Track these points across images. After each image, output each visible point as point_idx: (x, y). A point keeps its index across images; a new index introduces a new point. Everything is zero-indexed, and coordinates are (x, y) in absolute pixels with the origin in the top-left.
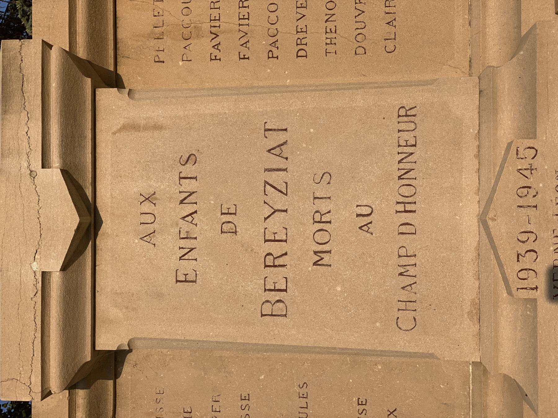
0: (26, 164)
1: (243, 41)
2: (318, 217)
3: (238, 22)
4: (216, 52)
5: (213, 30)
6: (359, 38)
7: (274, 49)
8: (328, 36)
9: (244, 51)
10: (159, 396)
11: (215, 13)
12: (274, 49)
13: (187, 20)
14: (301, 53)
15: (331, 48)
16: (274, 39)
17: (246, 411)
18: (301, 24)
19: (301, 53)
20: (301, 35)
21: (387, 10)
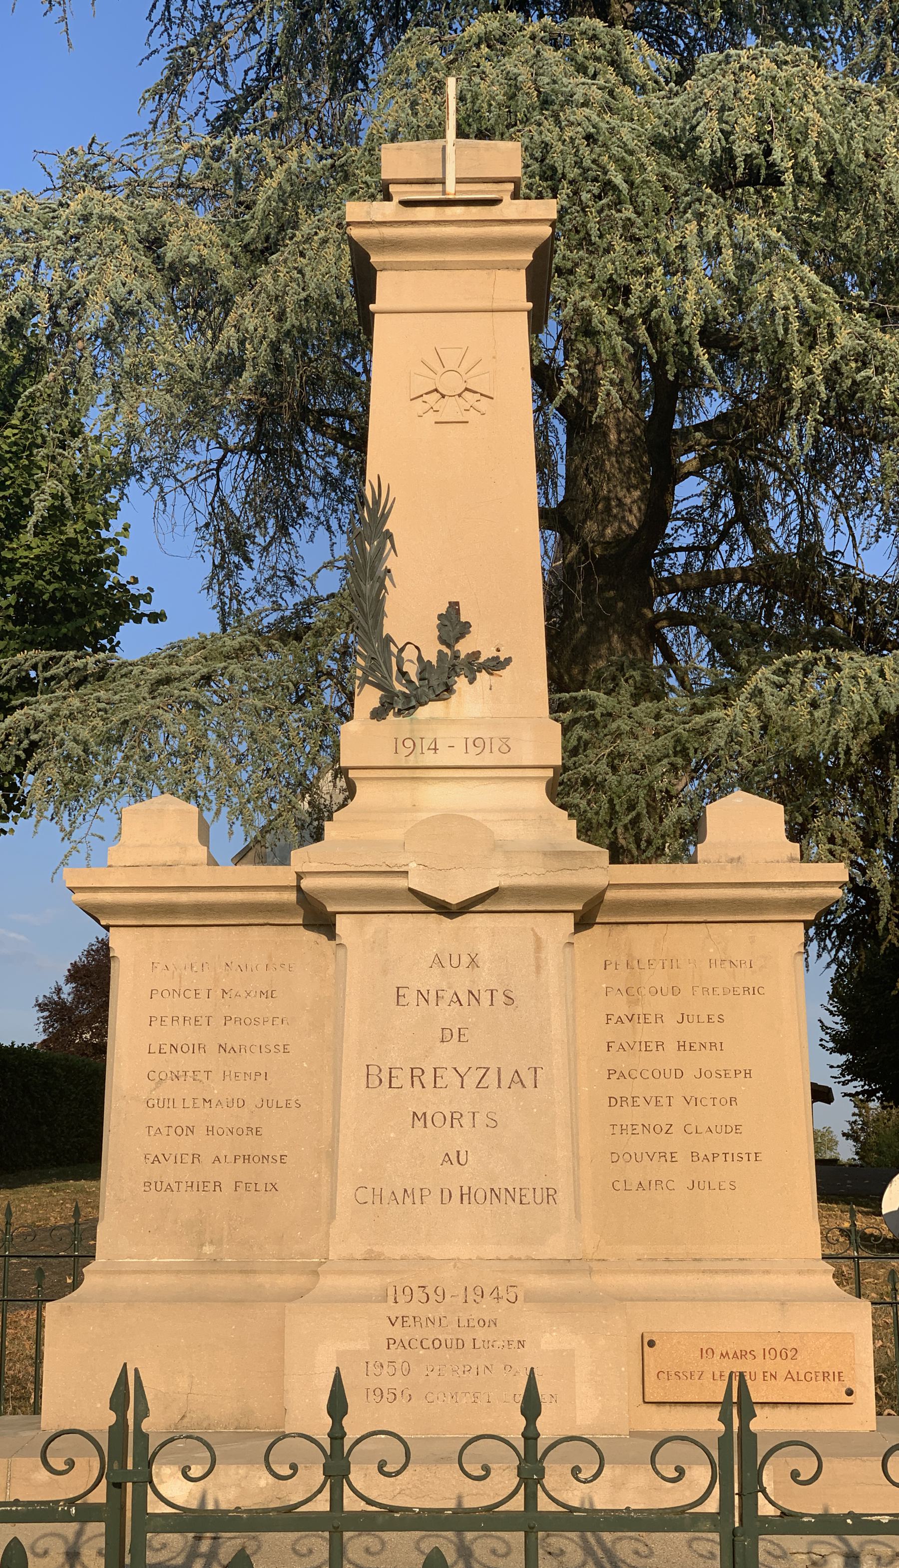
1: (626, 1046)
2: (456, 1116)
3: (643, 1040)
4: (614, 1019)
5: (636, 1017)
6: (627, 1156)
7: (617, 1075)
8: (630, 1127)
9: (615, 1047)
10: (287, 967)
11: (652, 1019)
12: (617, 1075)
13: (645, 991)
14: (613, 1101)
15: (617, 1129)
16: (627, 1075)
17: (273, 1050)
18: (640, 1101)
19: (613, 1101)
20: (630, 1101)
21: (653, 1183)
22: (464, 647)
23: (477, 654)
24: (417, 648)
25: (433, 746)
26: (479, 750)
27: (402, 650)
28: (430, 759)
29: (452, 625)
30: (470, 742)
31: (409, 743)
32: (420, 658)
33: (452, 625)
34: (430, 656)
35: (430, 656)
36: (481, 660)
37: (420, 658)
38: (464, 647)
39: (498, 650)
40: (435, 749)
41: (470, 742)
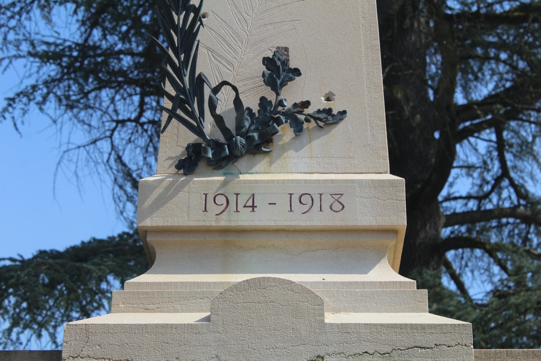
0: (331, 350)
22: (291, 95)
23: (306, 104)
24: (235, 89)
25: (250, 203)
26: (306, 208)
27: (216, 90)
28: (245, 219)
29: (278, 70)
30: (295, 199)
31: (221, 200)
32: (237, 102)
33: (278, 70)
34: (251, 102)
35: (251, 102)
36: (310, 110)
37: (237, 102)
38: (291, 95)
39: (328, 99)
40: (253, 207)
41: (295, 199)
